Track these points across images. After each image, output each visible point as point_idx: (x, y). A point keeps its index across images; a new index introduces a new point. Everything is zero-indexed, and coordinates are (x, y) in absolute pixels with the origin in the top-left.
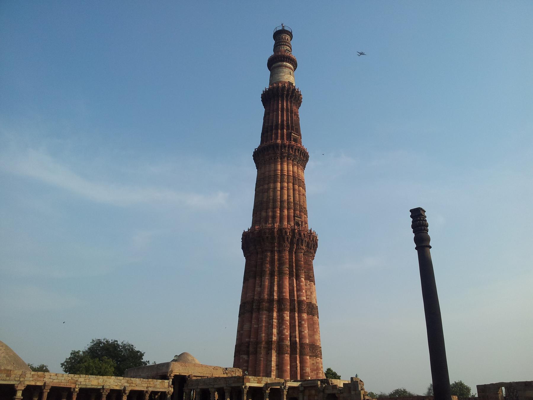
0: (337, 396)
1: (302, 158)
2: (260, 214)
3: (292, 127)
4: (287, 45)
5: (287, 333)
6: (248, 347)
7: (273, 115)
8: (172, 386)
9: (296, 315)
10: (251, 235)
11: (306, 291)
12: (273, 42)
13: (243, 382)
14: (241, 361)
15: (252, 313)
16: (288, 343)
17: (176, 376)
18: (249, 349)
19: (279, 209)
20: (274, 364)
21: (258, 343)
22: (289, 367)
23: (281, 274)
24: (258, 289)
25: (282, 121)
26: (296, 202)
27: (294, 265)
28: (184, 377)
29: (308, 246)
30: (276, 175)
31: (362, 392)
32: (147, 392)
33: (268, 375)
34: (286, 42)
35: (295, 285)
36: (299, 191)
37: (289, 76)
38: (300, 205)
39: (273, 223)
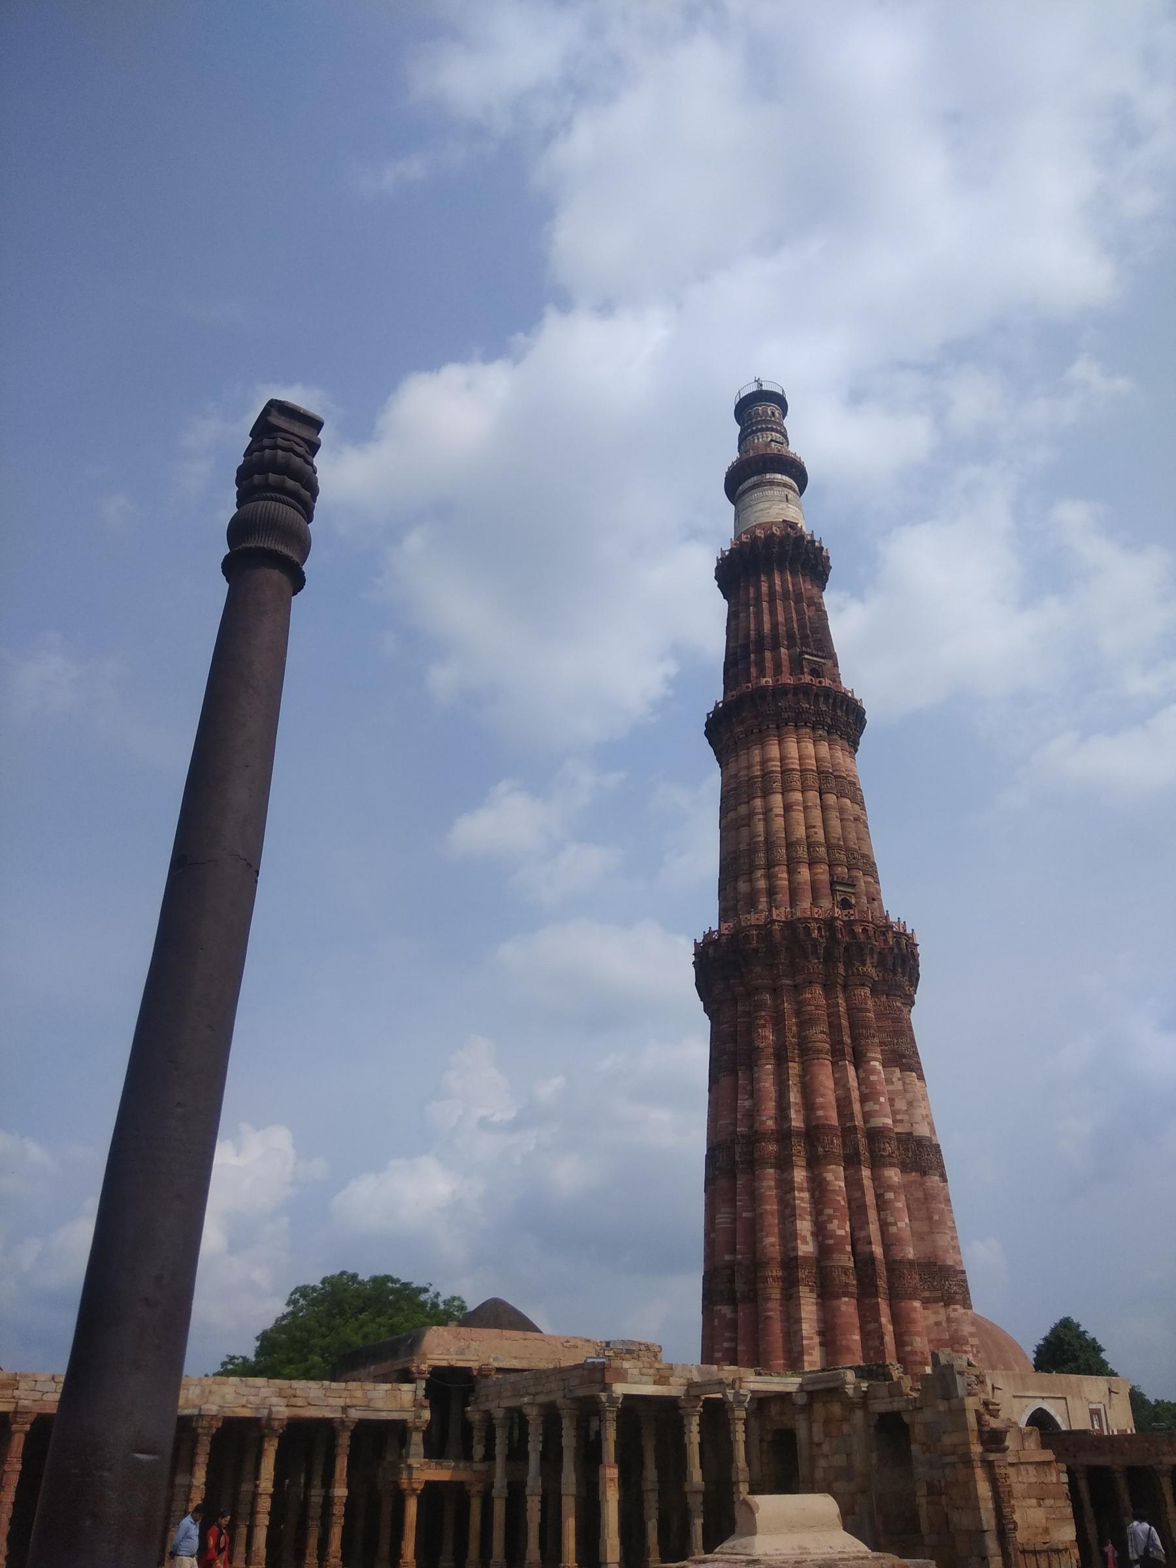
0: (906, 1418)
1: (844, 719)
2: (735, 888)
3: (804, 637)
4: (772, 430)
5: (841, 1229)
6: (731, 1280)
7: (748, 616)
8: (426, 1403)
9: (866, 1173)
10: (711, 951)
11: (891, 1101)
12: (737, 429)
13: (603, 1381)
14: (716, 1322)
15: (735, 1178)
16: (846, 1260)
17: (437, 1371)
18: (737, 1291)
19: (785, 868)
20: (809, 1327)
21: (756, 1265)
22: (857, 1337)
23: (806, 1052)
24: (744, 1103)
25: (775, 625)
26: (836, 841)
27: (845, 1023)
28: (468, 1370)
29: (881, 964)
30: (766, 775)
31: (972, 1404)
32: (342, 1422)
33: (794, 1364)
34: (766, 421)
35: (853, 1083)
36: (842, 810)
37: (784, 505)
38: (848, 850)
39: (772, 903)
